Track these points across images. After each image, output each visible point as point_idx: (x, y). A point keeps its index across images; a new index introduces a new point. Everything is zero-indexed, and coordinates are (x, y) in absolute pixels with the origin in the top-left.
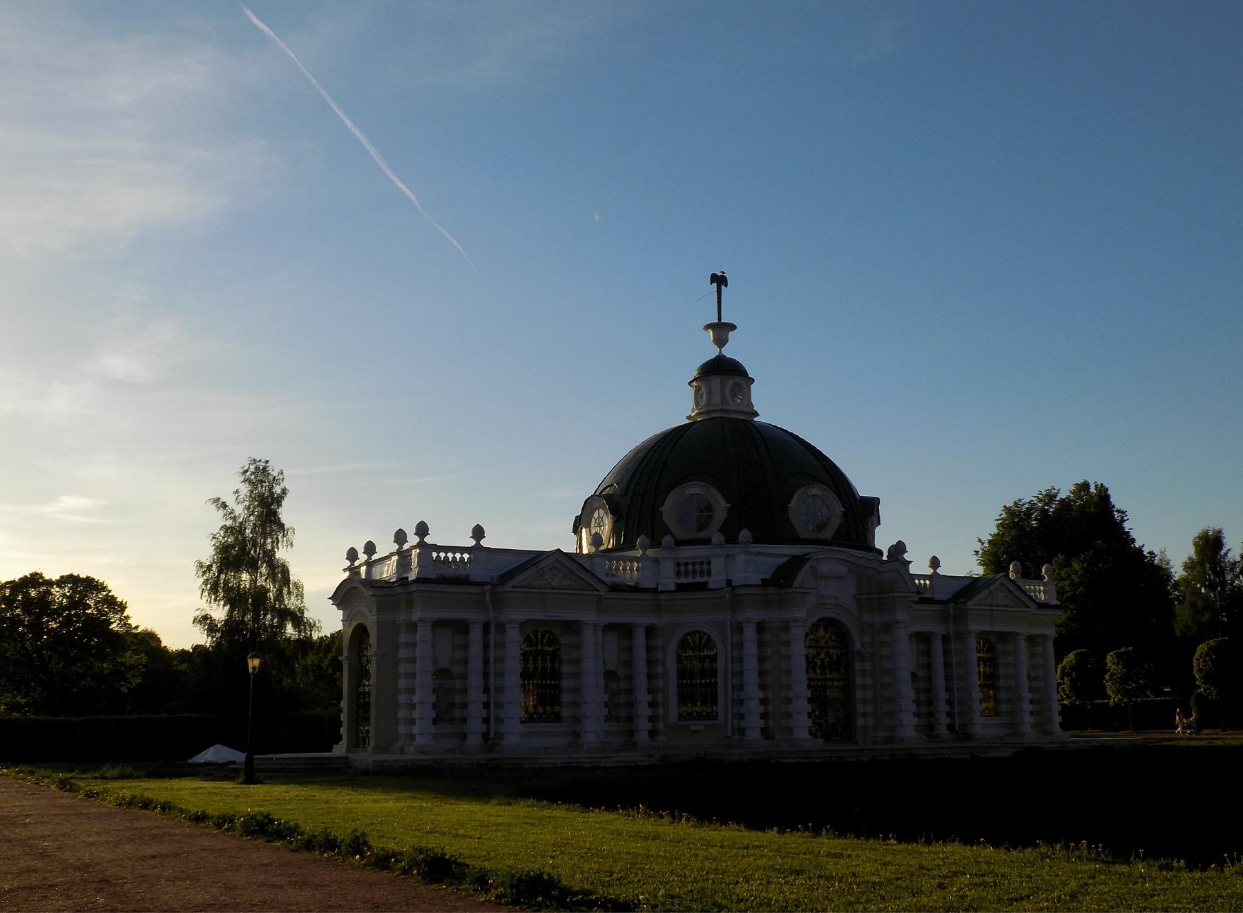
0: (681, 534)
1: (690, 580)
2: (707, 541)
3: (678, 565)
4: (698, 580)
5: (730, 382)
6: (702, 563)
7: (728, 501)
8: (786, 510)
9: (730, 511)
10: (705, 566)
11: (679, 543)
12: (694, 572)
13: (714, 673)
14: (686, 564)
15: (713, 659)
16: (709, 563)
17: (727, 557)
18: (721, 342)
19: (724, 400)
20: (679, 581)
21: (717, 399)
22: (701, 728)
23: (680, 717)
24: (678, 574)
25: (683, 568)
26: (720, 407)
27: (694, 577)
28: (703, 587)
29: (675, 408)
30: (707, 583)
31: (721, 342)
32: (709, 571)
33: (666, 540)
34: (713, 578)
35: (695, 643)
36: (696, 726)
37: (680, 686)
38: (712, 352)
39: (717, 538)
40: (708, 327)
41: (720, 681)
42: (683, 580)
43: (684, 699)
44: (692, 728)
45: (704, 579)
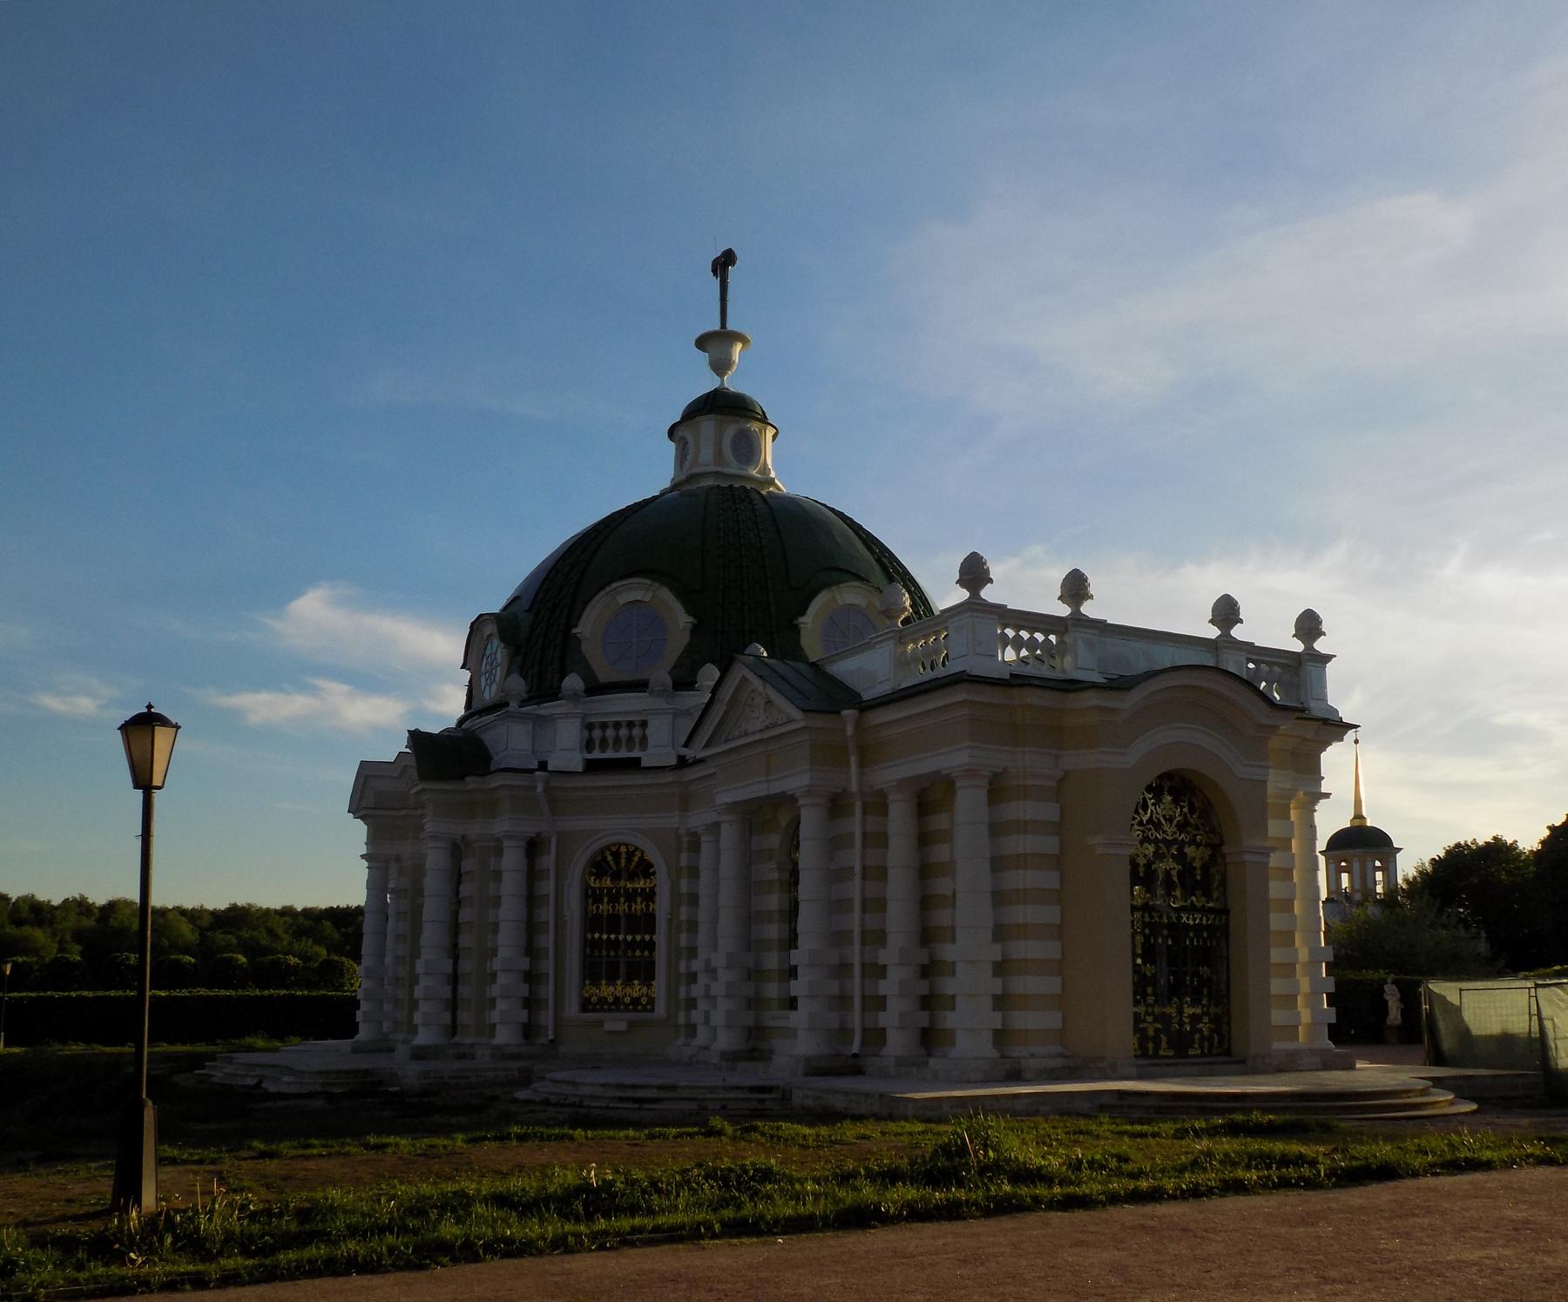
0: (604, 674)
1: (610, 754)
2: (640, 686)
3: (590, 727)
4: (623, 754)
5: (731, 431)
6: (631, 725)
7: (689, 613)
8: (796, 630)
9: (695, 630)
10: (637, 732)
11: (595, 688)
12: (617, 740)
13: (649, 922)
14: (604, 726)
15: (650, 896)
16: (644, 724)
17: (677, 714)
18: (721, 366)
19: (719, 454)
20: (589, 756)
21: (707, 455)
22: (622, 1026)
23: (586, 1006)
24: (589, 745)
25: (597, 733)
26: (713, 468)
27: (617, 748)
28: (633, 765)
29: (647, 472)
30: (639, 759)
31: (721, 366)
32: (644, 740)
33: (573, 682)
34: (650, 750)
35: (619, 867)
36: (615, 1022)
37: (589, 945)
38: (707, 383)
39: (661, 676)
40: (703, 342)
41: (660, 938)
42: (597, 754)
43: (592, 971)
44: (608, 1026)
45: (635, 754)
